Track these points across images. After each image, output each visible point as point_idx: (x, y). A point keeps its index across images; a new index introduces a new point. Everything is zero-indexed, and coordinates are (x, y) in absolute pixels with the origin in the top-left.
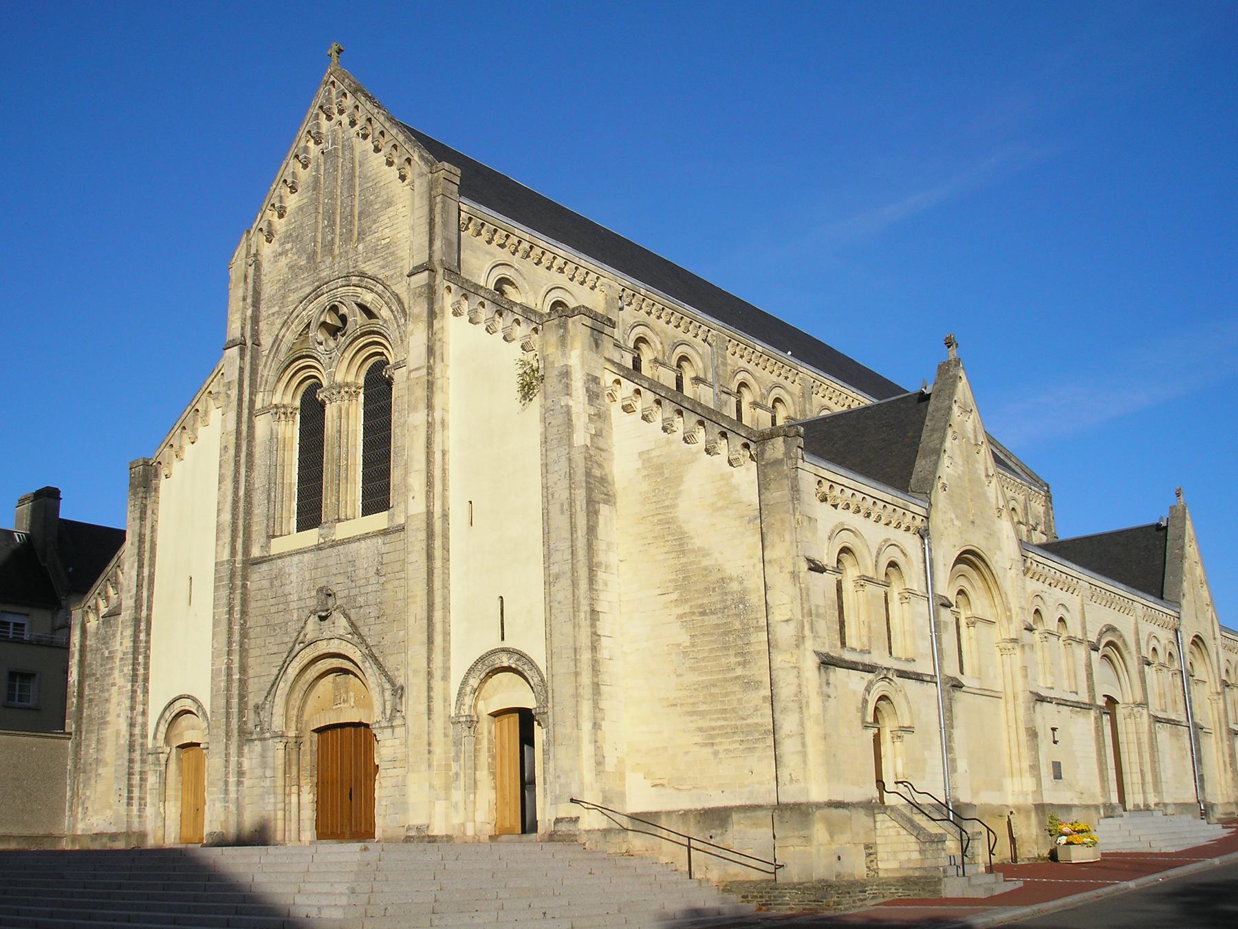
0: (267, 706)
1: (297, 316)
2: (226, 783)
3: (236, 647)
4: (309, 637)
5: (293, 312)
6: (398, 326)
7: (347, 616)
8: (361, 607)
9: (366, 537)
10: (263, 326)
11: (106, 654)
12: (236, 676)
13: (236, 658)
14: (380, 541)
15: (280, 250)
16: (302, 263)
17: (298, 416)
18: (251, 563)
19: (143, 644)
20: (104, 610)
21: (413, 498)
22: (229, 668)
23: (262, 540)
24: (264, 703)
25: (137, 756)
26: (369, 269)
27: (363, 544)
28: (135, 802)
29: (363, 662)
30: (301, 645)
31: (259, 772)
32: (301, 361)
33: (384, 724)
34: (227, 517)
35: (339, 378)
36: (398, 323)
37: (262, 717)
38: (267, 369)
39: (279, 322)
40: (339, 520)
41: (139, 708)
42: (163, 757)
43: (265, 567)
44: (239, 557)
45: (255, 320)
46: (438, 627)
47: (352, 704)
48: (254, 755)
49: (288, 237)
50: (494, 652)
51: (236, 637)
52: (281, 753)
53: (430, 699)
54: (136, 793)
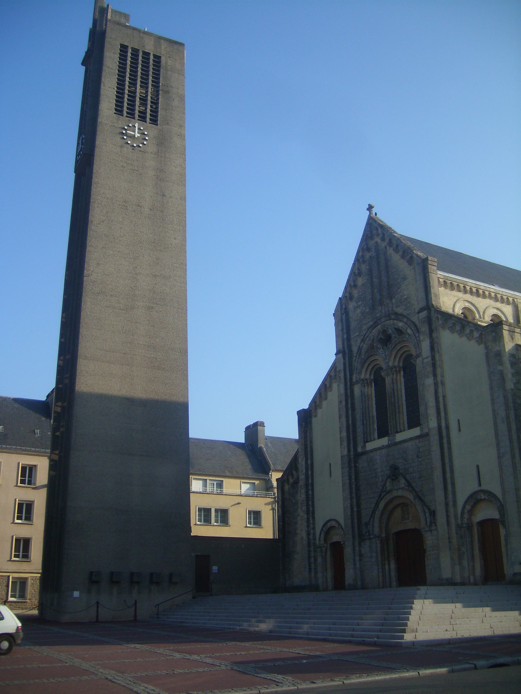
0: (371, 523)
1: (368, 337)
2: (354, 560)
3: (354, 495)
4: (388, 488)
5: (365, 334)
6: (416, 337)
7: (405, 478)
8: (411, 473)
9: (411, 439)
10: (353, 342)
11: (294, 501)
12: (355, 509)
13: (354, 501)
15: (356, 305)
16: (367, 311)
17: (373, 384)
18: (358, 455)
19: (311, 496)
20: (291, 481)
21: (431, 420)
22: (352, 506)
25: (312, 548)
26: (400, 310)
27: (409, 444)
28: (313, 571)
30: (385, 493)
33: (427, 529)
34: (344, 434)
36: (415, 336)
38: (356, 362)
39: (359, 340)
40: (397, 432)
41: (311, 526)
43: (364, 457)
44: (352, 453)
45: (349, 339)
46: (449, 481)
51: (354, 491)
52: (379, 545)
53: (448, 516)
54: (313, 566)
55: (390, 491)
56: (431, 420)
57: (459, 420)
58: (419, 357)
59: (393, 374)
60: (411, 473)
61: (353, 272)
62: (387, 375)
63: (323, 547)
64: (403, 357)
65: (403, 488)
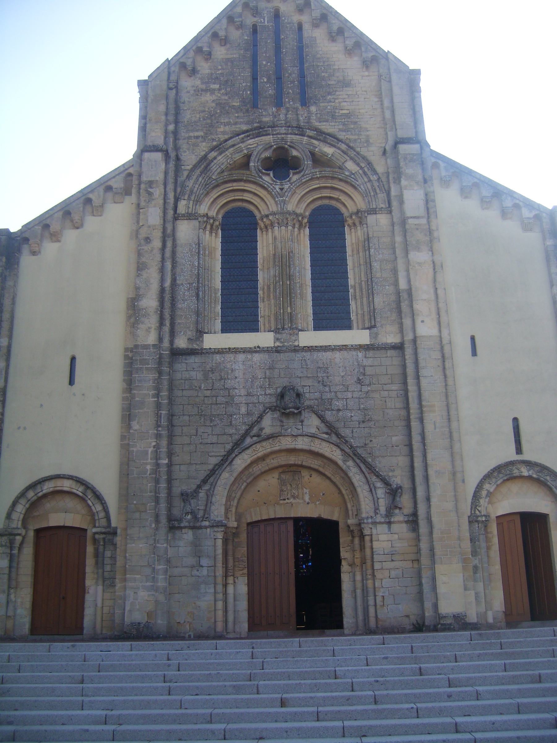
1: (234, 146)
4: (268, 431)
7: (321, 418)
8: (339, 410)
14: (360, 355)
17: (220, 232)
23: (190, 333)
24: (196, 491)
26: (326, 127)
27: (338, 355)
29: (344, 461)
30: (255, 438)
31: (191, 561)
32: (235, 184)
35: (290, 207)
37: (192, 505)
42: (19, 539)
43: (192, 360)
44: (166, 343)
47: (307, 498)
48: (181, 543)
49: (212, 78)
50: (512, 463)
52: (219, 543)
56: (423, 321)
57: (473, 338)
58: (376, 213)
59: (294, 227)
60: (339, 410)
61: (213, 31)
62: (278, 223)
63: (19, 535)
64: (313, 206)
65: (313, 436)
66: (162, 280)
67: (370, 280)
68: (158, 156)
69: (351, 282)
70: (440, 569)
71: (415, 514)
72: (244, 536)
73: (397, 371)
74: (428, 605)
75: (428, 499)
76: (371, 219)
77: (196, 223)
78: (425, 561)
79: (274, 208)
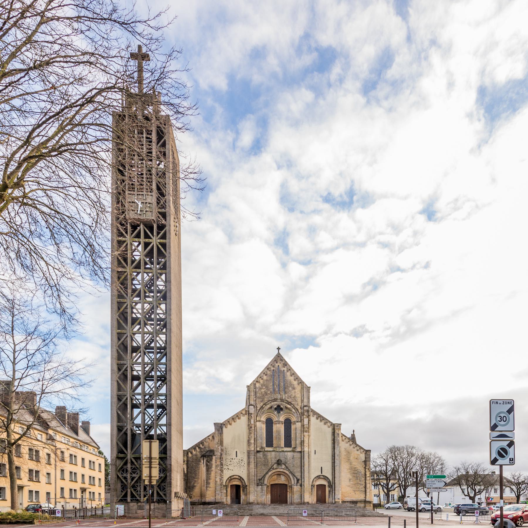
4: (275, 468)
7: (285, 466)
27: (289, 453)
31: (261, 491)
44: (256, 450)
50: (320, 475)
55: (276, 469)
65: (284, 469)
66: (254, 436)
67: (296, 437)
68: (253, 407)
69: (292, 437)
70: (305, 494)
71: (301, 484)
72: (270, 487)
73: (300, 457)
74: (303, 500)
75: (304, 482)
76: (297, 423)
77: (260, 423)
78: (303, 493)
79: (277, 420)
